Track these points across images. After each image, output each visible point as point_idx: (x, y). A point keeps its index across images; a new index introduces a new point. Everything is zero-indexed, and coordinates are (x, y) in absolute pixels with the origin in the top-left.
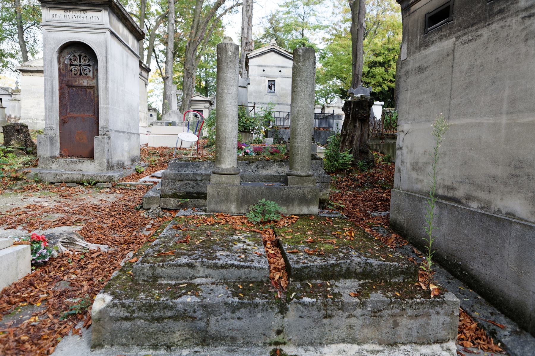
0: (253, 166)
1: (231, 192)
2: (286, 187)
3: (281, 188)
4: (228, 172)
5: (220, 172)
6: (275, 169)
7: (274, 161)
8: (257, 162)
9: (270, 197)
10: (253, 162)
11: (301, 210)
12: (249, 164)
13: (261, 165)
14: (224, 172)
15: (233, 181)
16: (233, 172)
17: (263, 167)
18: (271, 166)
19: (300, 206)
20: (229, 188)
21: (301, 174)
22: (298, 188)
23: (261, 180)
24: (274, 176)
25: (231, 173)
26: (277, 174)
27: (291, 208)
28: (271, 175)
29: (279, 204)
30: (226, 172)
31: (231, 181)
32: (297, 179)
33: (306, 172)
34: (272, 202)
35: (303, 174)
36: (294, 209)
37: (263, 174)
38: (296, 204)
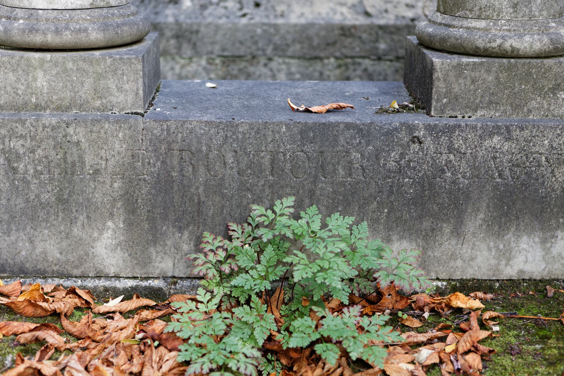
1: (89, 159)
2: (418, 120)
3: (390, 133)
4: (67, 38)
5: (17, 38)
9: (324, 186)
11: (507, 255)
14: (38, 39)
15: (98, 93)
16: (95, 36)
19: (499, 235)
20: (77, 133)
21: (512, 43)
22: (495, 130)
23: (281, 50)
24: (346, 31)
25: (82, 39)
26: (362, 20)
27: (446, 245)
28: (329, 27)
29: (374, 224)
30: (51, 39)
31: (86, 90)
32: (488, 73)
33: (544, 30)
34: (339, 223)
35: (530, 42)
36: (466, 251)
37: (294, 19)
38: (474, 223)
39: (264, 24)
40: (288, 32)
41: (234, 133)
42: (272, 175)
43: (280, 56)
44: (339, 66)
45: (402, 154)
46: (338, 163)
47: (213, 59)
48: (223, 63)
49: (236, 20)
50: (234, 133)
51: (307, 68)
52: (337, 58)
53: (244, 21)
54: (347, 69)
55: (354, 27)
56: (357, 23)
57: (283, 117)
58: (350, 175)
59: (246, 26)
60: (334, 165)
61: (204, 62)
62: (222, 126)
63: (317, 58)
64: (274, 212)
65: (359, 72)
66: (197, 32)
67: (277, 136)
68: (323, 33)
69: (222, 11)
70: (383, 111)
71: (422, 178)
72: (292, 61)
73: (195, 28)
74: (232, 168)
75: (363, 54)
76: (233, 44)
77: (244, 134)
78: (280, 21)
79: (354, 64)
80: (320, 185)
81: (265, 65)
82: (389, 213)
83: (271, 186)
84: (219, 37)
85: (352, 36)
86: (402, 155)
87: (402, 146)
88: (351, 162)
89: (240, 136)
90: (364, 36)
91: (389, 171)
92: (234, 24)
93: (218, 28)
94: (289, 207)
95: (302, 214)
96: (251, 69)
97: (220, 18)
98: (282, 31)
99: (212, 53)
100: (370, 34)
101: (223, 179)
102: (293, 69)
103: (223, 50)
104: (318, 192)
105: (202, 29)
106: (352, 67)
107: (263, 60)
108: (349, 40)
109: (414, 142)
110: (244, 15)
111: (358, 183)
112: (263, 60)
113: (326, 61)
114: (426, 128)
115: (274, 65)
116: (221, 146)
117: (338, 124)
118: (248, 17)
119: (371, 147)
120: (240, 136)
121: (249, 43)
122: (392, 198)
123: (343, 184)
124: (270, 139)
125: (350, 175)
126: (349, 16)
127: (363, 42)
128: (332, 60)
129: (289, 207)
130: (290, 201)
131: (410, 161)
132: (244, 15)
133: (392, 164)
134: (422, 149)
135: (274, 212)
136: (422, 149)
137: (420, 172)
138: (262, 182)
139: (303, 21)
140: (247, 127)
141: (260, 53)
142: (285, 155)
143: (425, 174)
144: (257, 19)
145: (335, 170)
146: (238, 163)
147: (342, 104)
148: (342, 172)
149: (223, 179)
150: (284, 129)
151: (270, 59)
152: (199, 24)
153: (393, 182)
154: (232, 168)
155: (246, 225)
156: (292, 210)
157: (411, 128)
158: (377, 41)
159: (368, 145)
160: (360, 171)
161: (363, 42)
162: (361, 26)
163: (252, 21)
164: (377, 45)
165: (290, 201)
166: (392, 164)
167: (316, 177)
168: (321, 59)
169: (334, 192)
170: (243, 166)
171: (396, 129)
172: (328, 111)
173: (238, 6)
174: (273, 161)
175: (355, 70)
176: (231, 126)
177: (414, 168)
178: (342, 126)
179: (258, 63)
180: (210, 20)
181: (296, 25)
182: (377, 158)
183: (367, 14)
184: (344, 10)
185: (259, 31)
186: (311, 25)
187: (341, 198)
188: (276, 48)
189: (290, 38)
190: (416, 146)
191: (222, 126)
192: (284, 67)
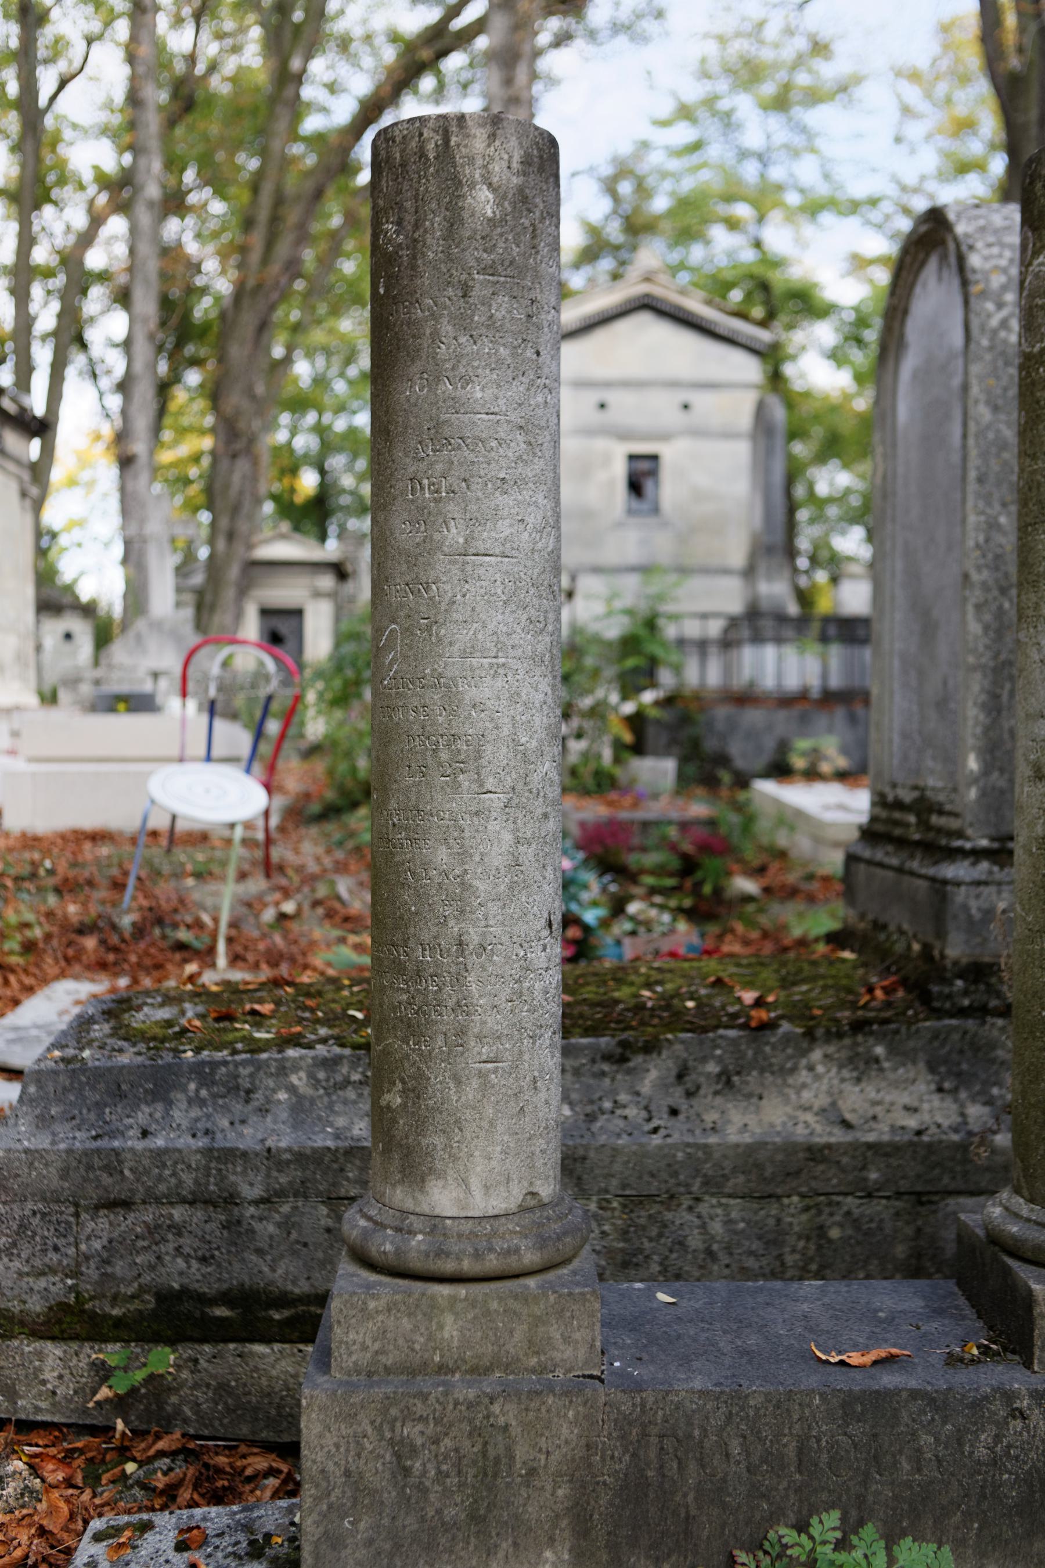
0: (652, 1075)
1: (521, 1453)
2: (1017, 1380)
3: (978, 1404)
4: (492, 1263)
5: (416, 1263)
6: (814, 1095)
7: (809, 1034)
8: (679, 1044)
10: (650, 1048)
12: (620, 1057)
13: (712, 1068)
14: (449, 1266)
15: (534, 1346)
16: (530, 1258)
17: (726, 1082)
18: (786, 1072)
20: (505, 1413)
23: (714, 1185)
24: (816, 1154)
25: (513, 1264)
26: (838, 1136)
28: (790, 1148)
30: (467, 1266)
31: (516, 1342)
37: (733, 1136)
39: (688, 1145)
40: (725, 1156)
41: (742, 1409)
42: (800, 1472)
43: (713, 1195)
44: (806, 1209)
45: (996, 1436)
46: (901, 1452)
47: (608, 1201)
48: (625, 1206)
49: (644, 1140)
50: (742, 1409)
51: (756, 1213)
52: (803, 1196)
53: (656, 1140)
54: (820, 1213)
55: (829, 1146)
56: (833, 1140)
57: (812, 1380)
58: (919, 1470)
59: (660, 1148)
60: (894, 1456)
61: (593, 1207)
62: (724, 1398)
63: (770, 1196)
64: (811, 1538)
65: (837, 1218)
66: (584, 1158)
67: (807, 1411)
68: (780, 1157)
69: (621, 1123)
70: (953, 1361)
71: (1029, 1472)
72: (732, 1202)
73: (581, 1152)
74: (739, 1463)
75: (842, 1189)
76: (640, 1178)
77: (757, 1409)
78: (713, 1140)
79: (830, 1204)
80: (874, 1487)
81: (690, 1209)
82: (980, 1529)
83: (798, 1490)
84: (617, 1167)
85: (824, 1160)
86: (997, 1438)
87: (997, 1423)
88: (919, 1450)
89: (752, 1413)
90: (845, 1160)
91: (978, 1462)
92: (641, 1145)
93: (616, 1151)
94: (834, 1529)
95: (854, 1540)
96: (668, 1216)
97: (619, 1136)
98: (717, 1155)
99: (607, 1191)
100: (853, 1157)
101: (724, 1480)
102: (734, 1215)
103: (624, 1186)
104: (870, 1498)
105: (592, 1154)
106: (827, 1210)
107: (686, 1202)
108: (821, 1167)
109: (1014, 1418)
110: (655, 1130)
111: (932, 1482)
112: (686, 1202)
113: (786, 1201)
114: (1031, 1396)
115: (703, 1208)
116: (722, 1429)
117: (897, 1392)
118: (662, 1132)
119: (949, 1427)
120: (752, 1413)
121: (664, 1175)
122: (985, 1506)
123: (908, 1485)
124: (796, 1417)
125: (919, 1470)
126: (819, 1128)
127: (843, 1171)
128: (795, 1199)
129: (834, 1529)
130: (832, 1519)
131: (1009, 1446)
132: (655, 1130)
133: (981, 1452)
134: (1027, 1428)
135: (811, 1538)
136: (1027, 1428)
137: (1025, 1463)
138: (785, 1484)
139: (747, 1139)
140: (761, 1399)
141: (682, 1189)
142: (818, 1441)
143: (1034, 1466)
144: (676, 1138)
145: (895, 1463)
146: (748, 1454)
147: (894, 1351)
148: (906, 1466)
149: (724, 1480)
150: (817, 1401)
151: (698, 1200)
152: (587, 1147)
153: (985, 1480)
154: (739, 1463)
155: (760, 1554)
156: (838, 1534)
157: (1009, 1397)
158: (864, 1168)
159: (944, 1423)
160: (934, 1463)
161: (843, 1171)
162: (839, 1144)
163: (669, 1140)
164: (864, 1173)
165: (832, 1519)
166: (981, 1452)
167: (867, 1475)
168: (778, 1198)
169: (895, 1497)
170: (755, 1459)
171: (986, 1398)
172: (875, 1363)
173: (644, 1114)
174: (800, 1451)
175: (831, 1214)
176: (739, 1397)
177: (1017, 1457)
178: (904, 1395)
179: (679, 1205)
180: (603, 1139)
181: (737, 1146)
182: (960, 1443)
183: (846, 1125)
184: (809, 1117)
185: (680, 1155)
186: (761, 1145)
187: (906, 1507)
188: (705, 1184)
189: (728, 1165)
190: (1018, 1424)
191: (724, 1398)
192: (719, 1211)
